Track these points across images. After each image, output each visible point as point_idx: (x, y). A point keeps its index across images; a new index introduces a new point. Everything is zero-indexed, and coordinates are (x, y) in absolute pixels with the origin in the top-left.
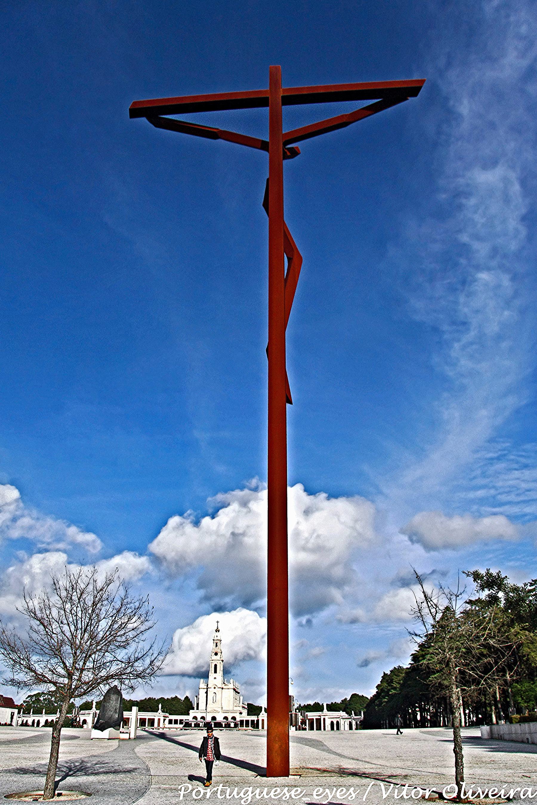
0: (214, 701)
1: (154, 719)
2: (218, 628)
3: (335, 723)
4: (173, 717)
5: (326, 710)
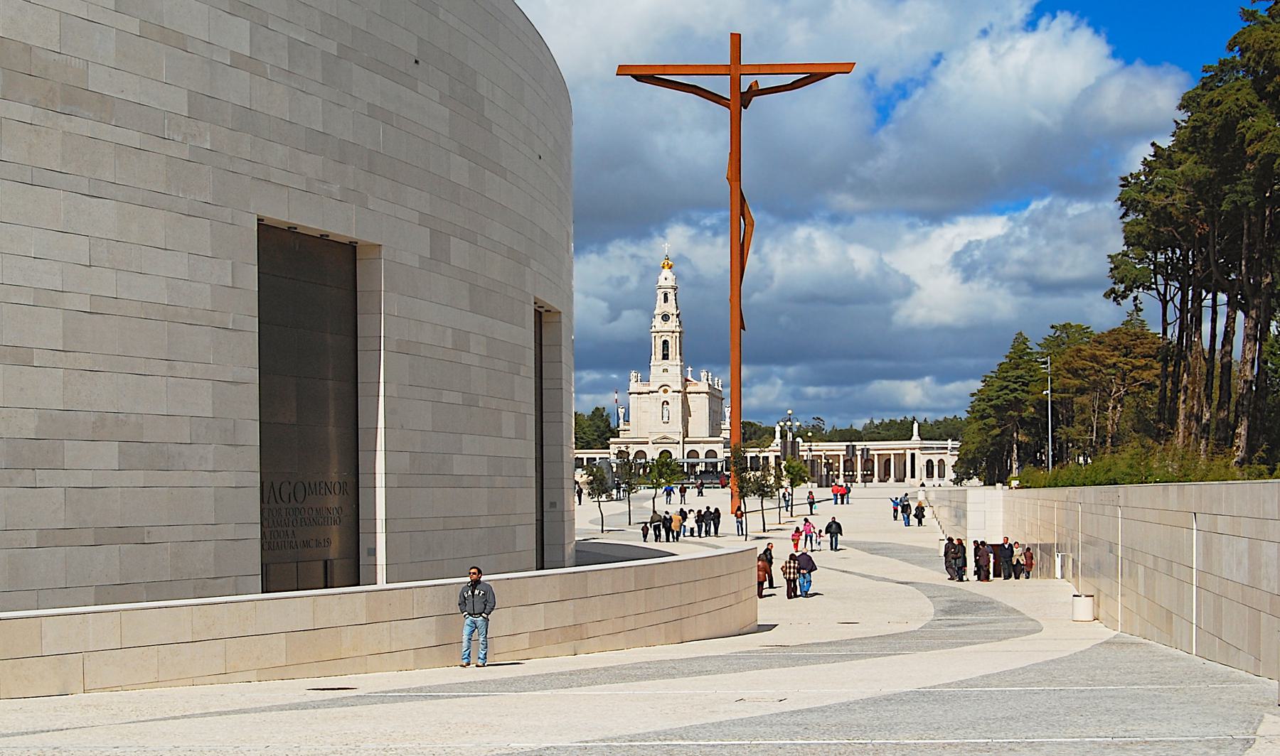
0: (666, 419)
3: (936, 463)
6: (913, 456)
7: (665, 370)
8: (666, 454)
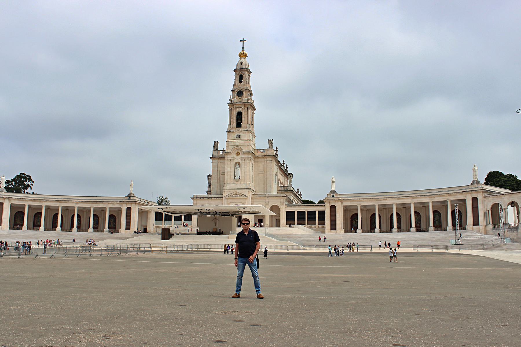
0: (237, 177)
2: (243, 50)
6: (475, 200)
7: (238, 137)
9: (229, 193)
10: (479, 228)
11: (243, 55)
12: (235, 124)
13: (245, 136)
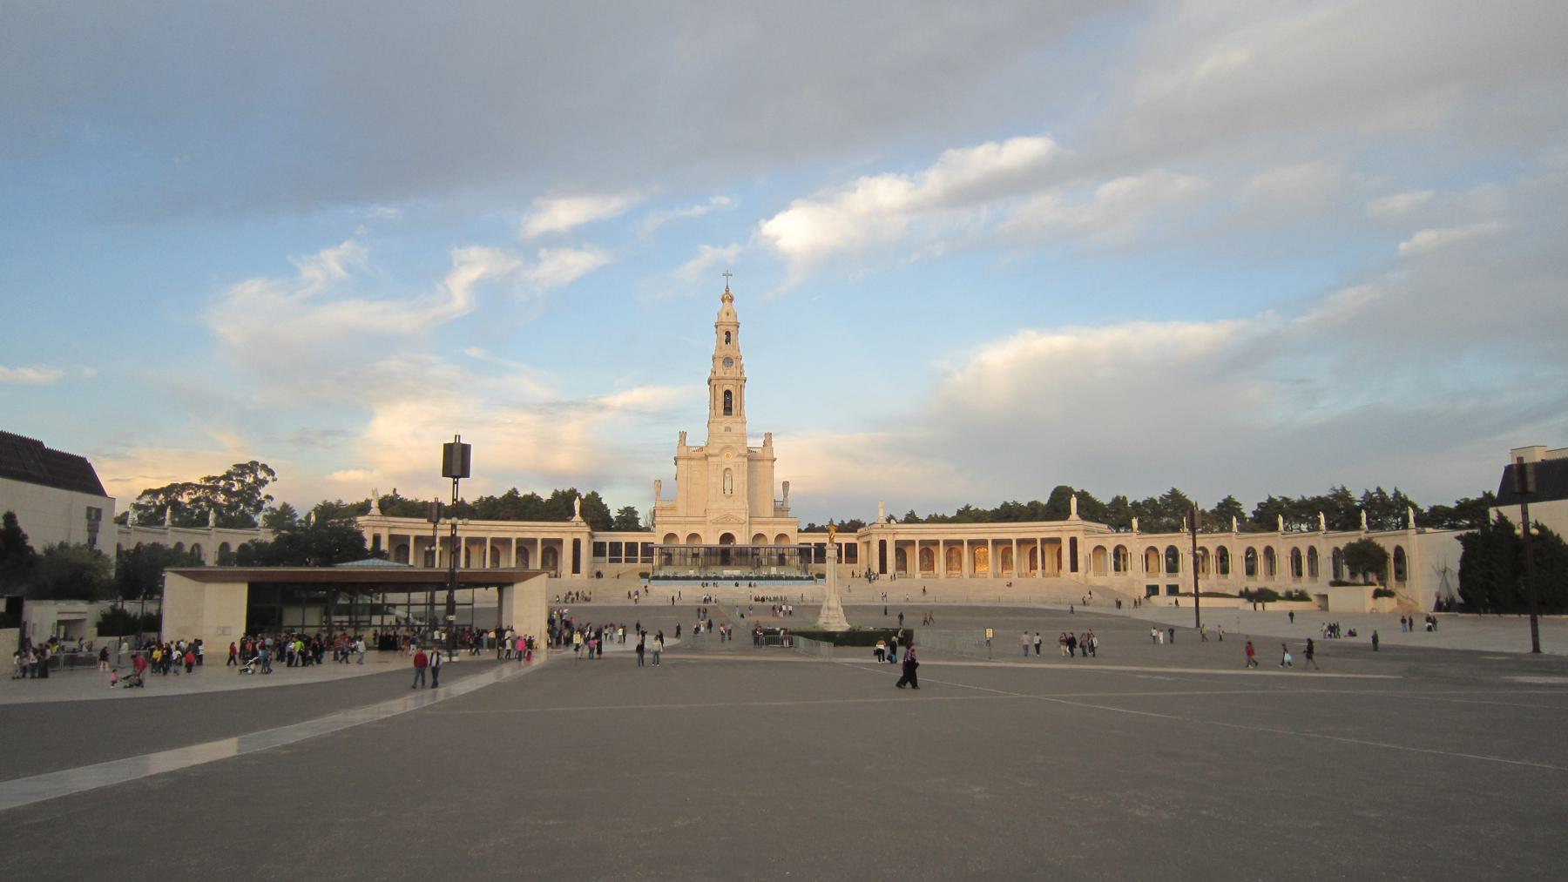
0: (728, 492)
1: (560, 542)
4: (607, 537)
5: (1077, 517)
6: (1073, 542)
7: (728, 429)
8: (727, 538)
9: (716, 516)
10: (1077, 576)
11: (728, 298)
12: (721, 410)
13: (736, 428)
